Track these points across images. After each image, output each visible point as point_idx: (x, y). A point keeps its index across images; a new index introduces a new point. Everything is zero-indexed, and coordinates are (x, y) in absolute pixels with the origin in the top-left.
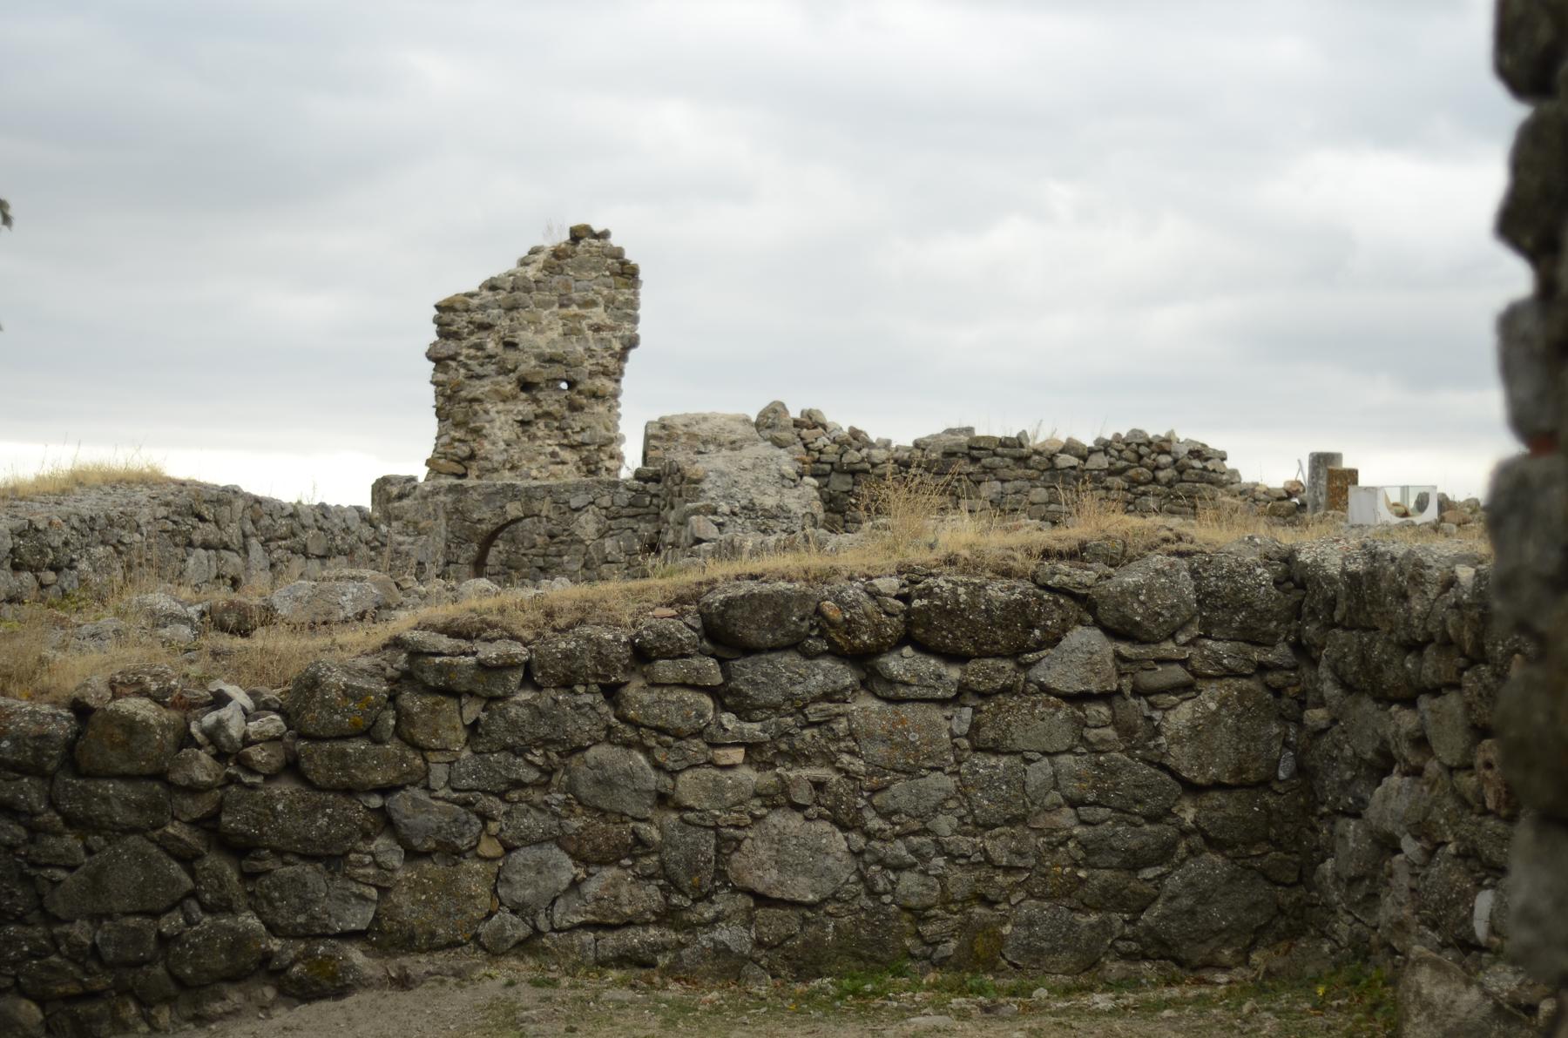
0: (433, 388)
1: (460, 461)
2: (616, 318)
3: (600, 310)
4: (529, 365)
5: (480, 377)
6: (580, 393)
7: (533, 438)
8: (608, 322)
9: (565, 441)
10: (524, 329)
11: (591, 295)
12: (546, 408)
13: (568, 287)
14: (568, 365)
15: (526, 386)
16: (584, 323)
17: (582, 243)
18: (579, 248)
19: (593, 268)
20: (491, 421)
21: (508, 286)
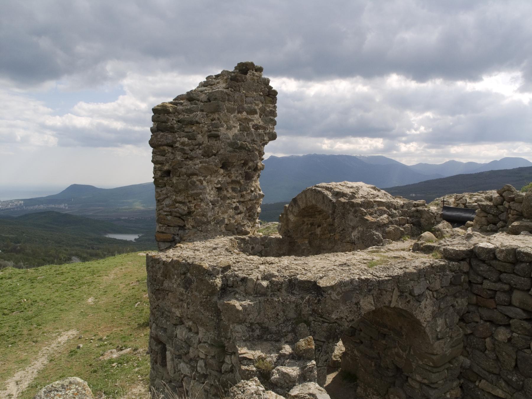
0: (152, 165)
1: (181, 217)
2: (265, 122)
3: (257, 116)
4: (224, 150)
5: (191, 159)
6: (249, 168)
7: (224, 198)
8: (261, 123)
9: (242, 200)
10: (222, 126)
11: (254, 106)
12: (234, 178)
13: (242, 101)
14: (249, 150)
15: (225, 165)
16: (251, 125)
17: (249, 73)
18: (248, 76)
19: (255, 91)
20: (205, 188)
21: (203, 97)
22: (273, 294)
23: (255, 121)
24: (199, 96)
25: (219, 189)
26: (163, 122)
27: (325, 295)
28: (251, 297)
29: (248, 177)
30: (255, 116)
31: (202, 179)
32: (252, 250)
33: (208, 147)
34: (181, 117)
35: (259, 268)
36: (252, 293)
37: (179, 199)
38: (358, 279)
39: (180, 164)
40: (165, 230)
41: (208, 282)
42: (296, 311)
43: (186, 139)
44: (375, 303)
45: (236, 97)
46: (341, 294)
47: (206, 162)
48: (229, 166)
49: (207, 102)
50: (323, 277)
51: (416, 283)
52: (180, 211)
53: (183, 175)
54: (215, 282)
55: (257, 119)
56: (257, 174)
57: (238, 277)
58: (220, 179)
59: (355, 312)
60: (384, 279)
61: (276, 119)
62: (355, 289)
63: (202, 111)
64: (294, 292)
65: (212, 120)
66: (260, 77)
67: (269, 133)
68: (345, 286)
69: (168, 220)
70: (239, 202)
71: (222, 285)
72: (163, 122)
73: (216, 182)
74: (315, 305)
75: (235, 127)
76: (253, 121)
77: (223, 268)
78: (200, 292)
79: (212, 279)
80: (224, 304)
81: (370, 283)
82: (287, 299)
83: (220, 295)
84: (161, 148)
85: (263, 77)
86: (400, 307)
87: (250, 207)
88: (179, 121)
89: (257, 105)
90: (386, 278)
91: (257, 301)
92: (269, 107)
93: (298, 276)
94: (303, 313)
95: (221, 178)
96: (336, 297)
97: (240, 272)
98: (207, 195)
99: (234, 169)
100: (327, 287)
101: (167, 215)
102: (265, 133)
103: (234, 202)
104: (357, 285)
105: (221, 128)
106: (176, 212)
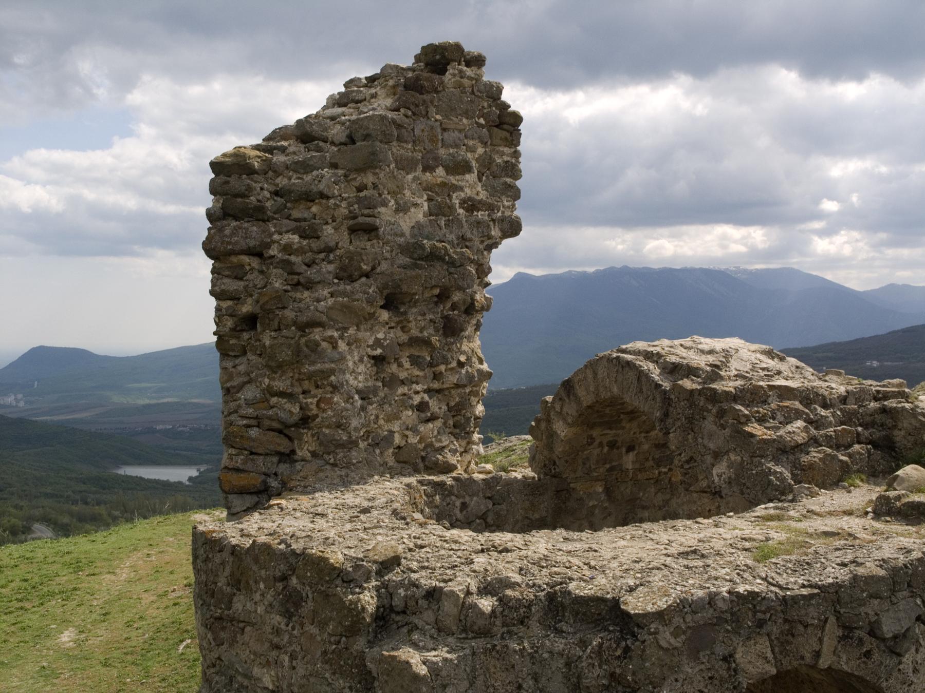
0: (213, 302)
1: (283, 430)
2: (493, 191)
3: (471, 178)
5: (309, 285)
6: (454, 307)
7: (392, 382)
8: (483, 195)
9: (436, 385)
10: (385, 204)
12: (415, 332)
13: (433, 140)
14: (452, 263)
17: (450, 71)
18: (447, 77)
19: (467, 114)
20: (342, 359)
21: (337, 132)
22: (509, 632)
23: (467, 190)
24: (326, 130)
25: (378, 361)
26: (237, 195)
27: (643, 635)
28: (450, 639)
29: (451, 330)
30: (467, 176)
31: (336, 334)
32: (461, 511)
33: (351, 256)
34: (282, 181)
35: (472, 562)
36: (454, 628)
37: (280, 384)
38: (729, 592)
39: (281, 301)
40: (245, 462)
41: (341, 599)
42: (567, 677)
43: (296, 238)
44: (775, 658)
45: (417, 132)
46: (684, 633)
47: (344, 294)
48: (404, 304)
49: (345, 144)
50: (637, 586)
51: (886, 605)
52: (282, 415)
53: (287, 327)
54: (359, 600)
55: (471, 186)
56: (474, 322)
57: (417, 586)
58: (380, 336)
59: (721, 679)
60: (797, 592)
61: (518, 183)
62: (721, 620)
63: (334, 166)
64: (563, 626)
65: (359, 189)
66: (478, 79)
67: (502, 220)
68: (694, 612)
69: (250, 438)
70: (428, 391)
71: (378, 608)
72: (237, 195)
73: (371, 343)
74: (616, 663)
75: (416, 205)
76: (461, 189)
77: (382, 563)
78: (323, 625)
79: (353, 593)
80: (382, 660)
81: (760, 602)
82: (543, 645)
83: (372, 635)
84: (234, 259)
85: (485, 79)
86: (845, 668)
87: (457, 404)
88: (276, 193)
89: (472, 150)
90: (804, 592)
91: (467, 651)
92: (503, 154)
93: (572, 586)
94: (585, 682)
95: (382, 332)
96: (672, 641)
97: (423, 573)
98: (348, 376)
99: (414, 310)
100: (646, 615)
101: (248, 426)
102: (493, 220)
103: (417, 393)
104: (725, 608)
105: (382, 210)
106: (270, 418)
